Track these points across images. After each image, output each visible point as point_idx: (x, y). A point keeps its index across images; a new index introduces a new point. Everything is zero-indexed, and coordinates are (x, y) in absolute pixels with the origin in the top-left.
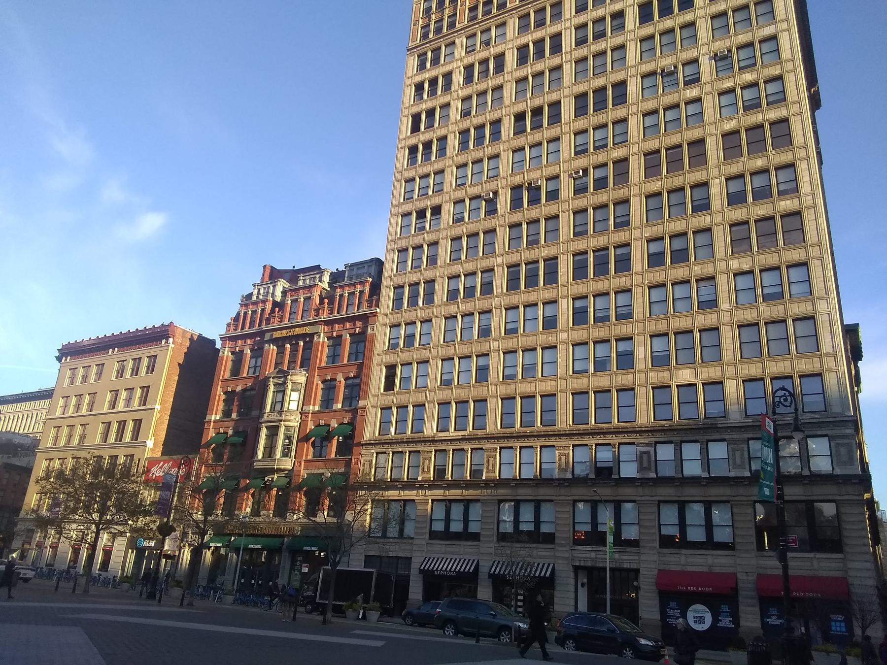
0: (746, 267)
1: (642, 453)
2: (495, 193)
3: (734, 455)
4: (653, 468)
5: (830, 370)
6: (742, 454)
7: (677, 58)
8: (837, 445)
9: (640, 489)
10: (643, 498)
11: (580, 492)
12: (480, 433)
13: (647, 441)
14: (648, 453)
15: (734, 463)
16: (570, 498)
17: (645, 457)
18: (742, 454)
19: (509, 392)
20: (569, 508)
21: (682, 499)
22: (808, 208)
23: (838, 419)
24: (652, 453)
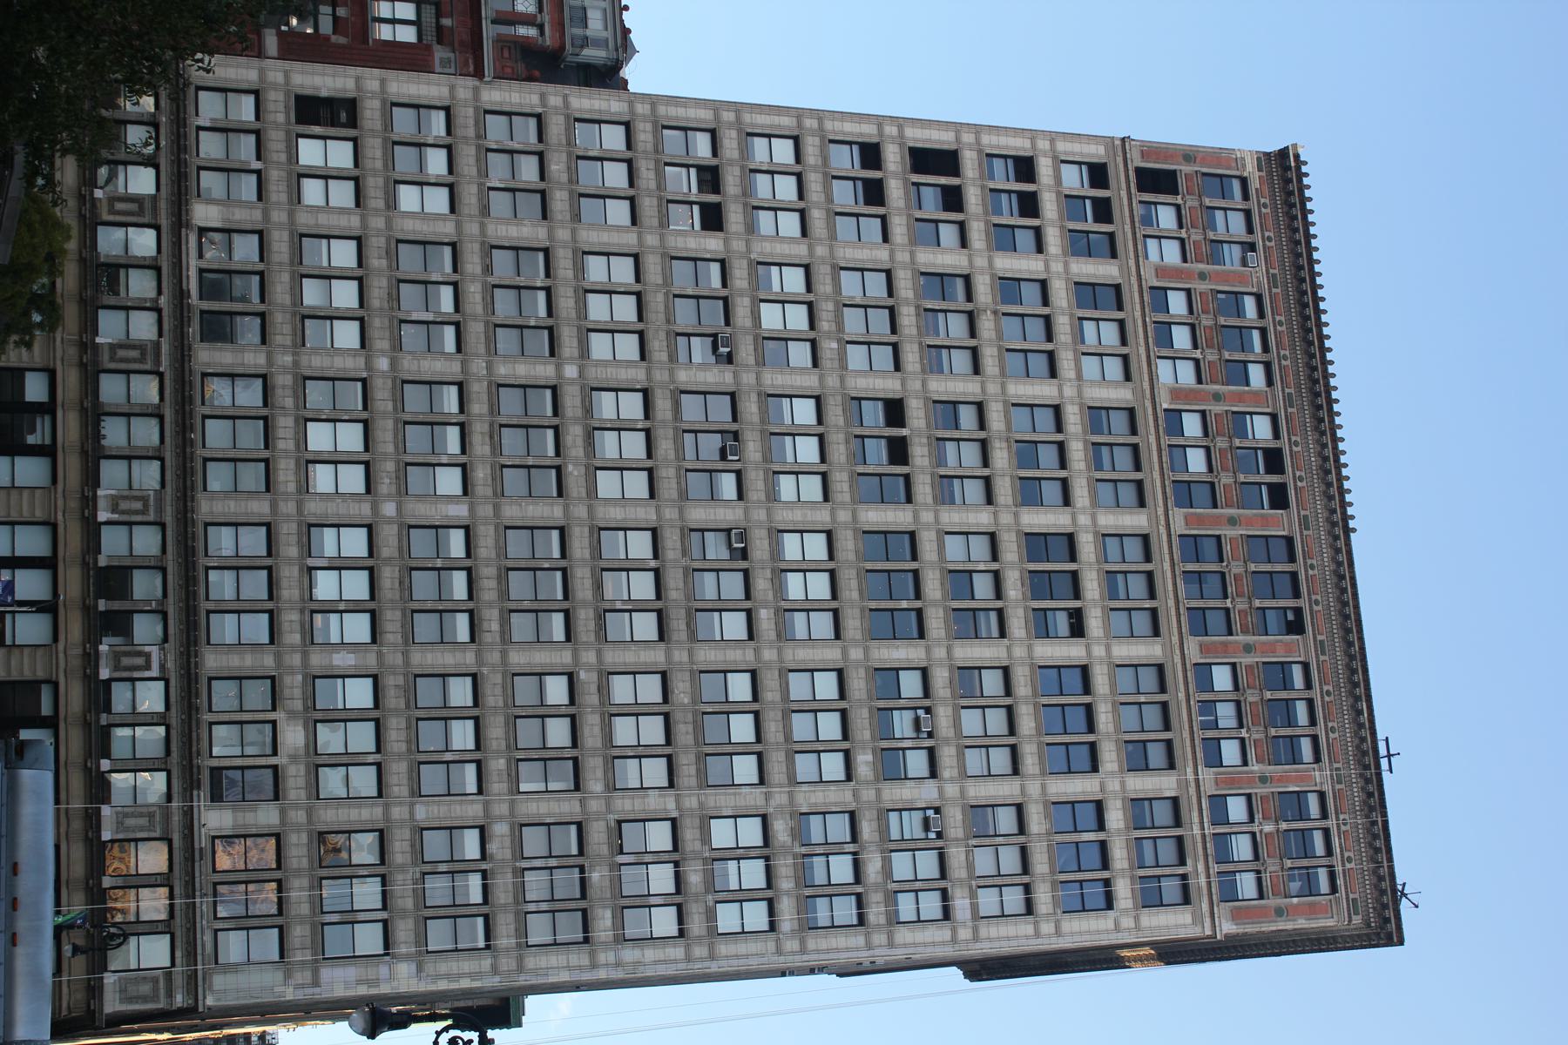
0: (492, 847)
1: (148, 656)
2: (730, 359)
3: (141, 815)
4: (117, 675)
5: (288, 975)
6: (142, 829)
7: (947, 741)
8: (155, 980)
9: (79, 651)
10: (61, 655)
11: (72, 539)
12: (194, 330)
13: (170, 665)
14: (148, 667)
15: (126, 815)
16: (60, 517)
17: (140, 661)
18: (142, 829)
19: (279, 392)
20: (39, 514)
21: (62, 725)
22: (592, 955)
23: (200, 983)
24: (147, 674)
